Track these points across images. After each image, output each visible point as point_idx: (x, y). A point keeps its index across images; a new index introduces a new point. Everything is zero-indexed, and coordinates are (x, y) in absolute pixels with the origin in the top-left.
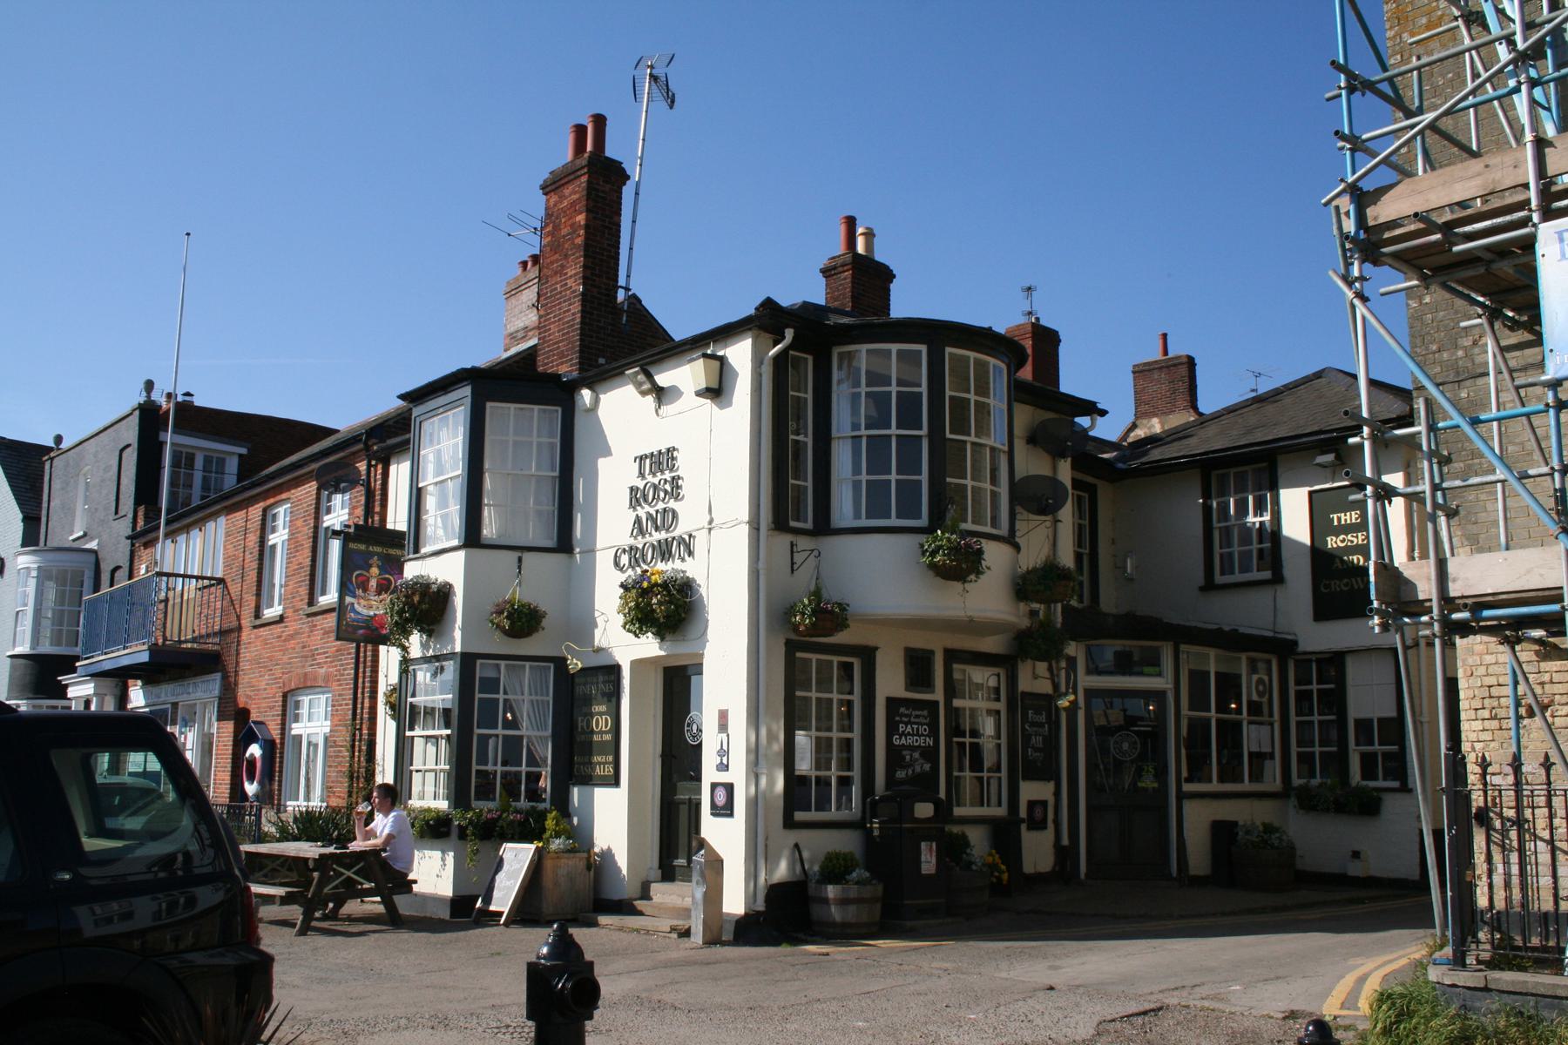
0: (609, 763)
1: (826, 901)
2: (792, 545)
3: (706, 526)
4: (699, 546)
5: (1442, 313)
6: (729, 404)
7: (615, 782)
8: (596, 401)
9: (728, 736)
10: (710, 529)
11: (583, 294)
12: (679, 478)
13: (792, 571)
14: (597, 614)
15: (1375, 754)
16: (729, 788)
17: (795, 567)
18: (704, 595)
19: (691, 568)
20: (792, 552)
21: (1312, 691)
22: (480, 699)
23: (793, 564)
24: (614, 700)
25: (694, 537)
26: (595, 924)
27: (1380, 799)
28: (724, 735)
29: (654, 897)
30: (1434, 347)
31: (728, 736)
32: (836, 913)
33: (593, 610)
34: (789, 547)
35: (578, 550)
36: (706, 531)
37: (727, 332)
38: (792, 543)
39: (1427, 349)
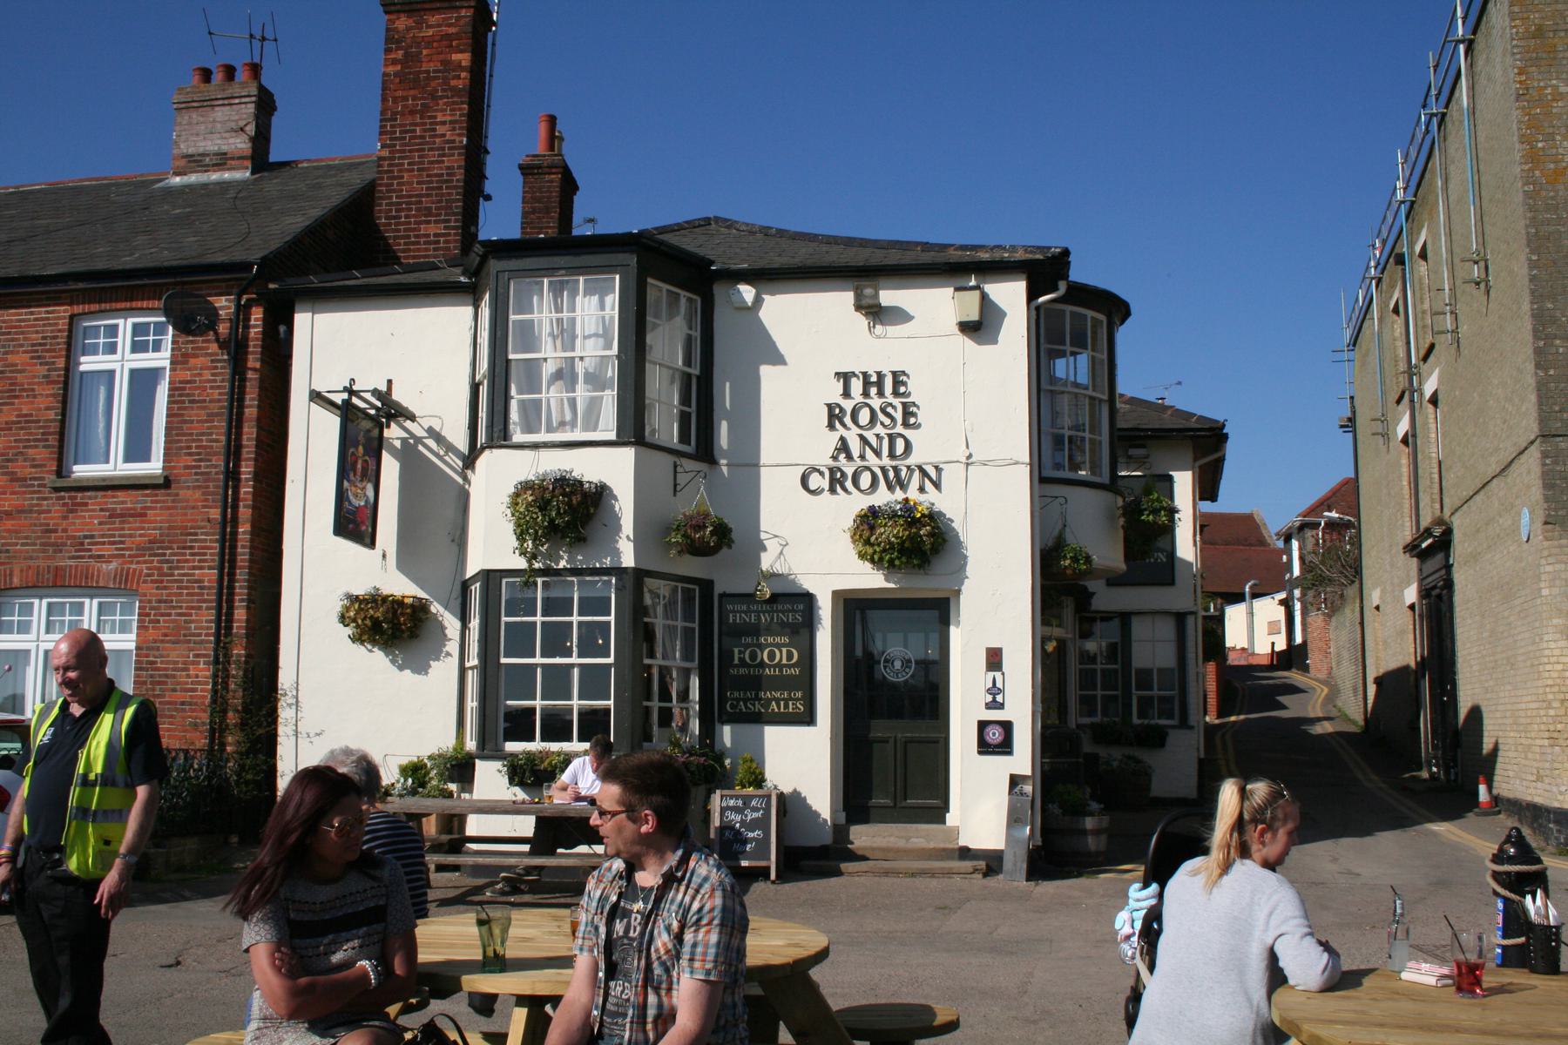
0: (798, 699)
1: (1084, 832)
2: (675, 466)
3: (964, 460)
4: (951, 476)
5: (1563, 385)
6: (993, 340)
7: (808, 718)
8: (758, 301)
9: (1003, 674)
10: (968, 464)
11: (466, 147)
12: (914, 404)
13: (675, 491)
14: (763, 536)
15: (1151, 698)
16: (1007, 727)
17: (678, 488)
18: (959, 530)
19: (945, 502)
20: (675, 472)
21: (571, 623)
22: (609, 615)
23: (675, 485)
24: (805, 632)
25: (941, 469)
26: (839, 873)
27: (1167, 734)
28: (998, 675)
29: (855, 841)
30: (1557, 408)
31: (1003, 674)
32: (1092, 843)
33: (757, 530)
34: (672, 469)
35: (723, 462)
36: (963, 467)
37: (999, 268)
38: (675, 463)
39: (1551, 408)
